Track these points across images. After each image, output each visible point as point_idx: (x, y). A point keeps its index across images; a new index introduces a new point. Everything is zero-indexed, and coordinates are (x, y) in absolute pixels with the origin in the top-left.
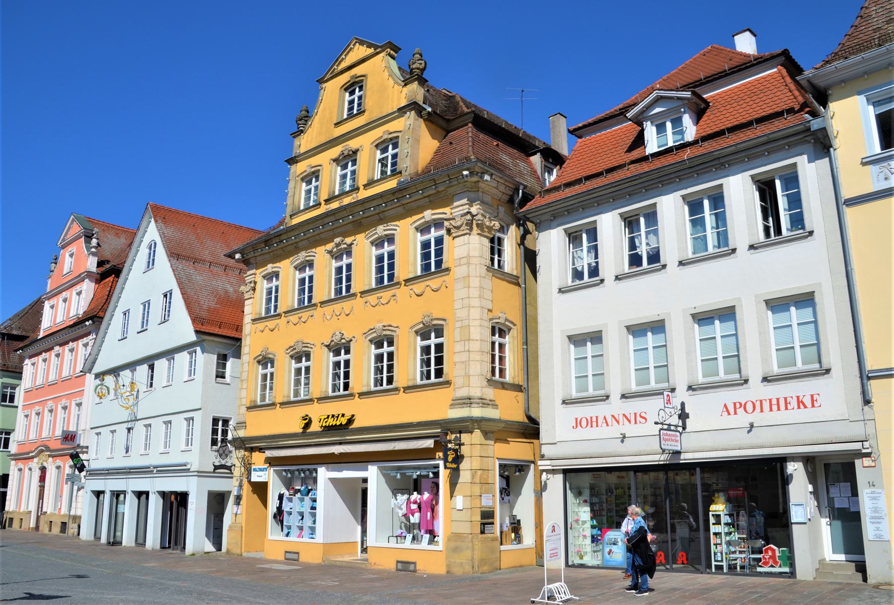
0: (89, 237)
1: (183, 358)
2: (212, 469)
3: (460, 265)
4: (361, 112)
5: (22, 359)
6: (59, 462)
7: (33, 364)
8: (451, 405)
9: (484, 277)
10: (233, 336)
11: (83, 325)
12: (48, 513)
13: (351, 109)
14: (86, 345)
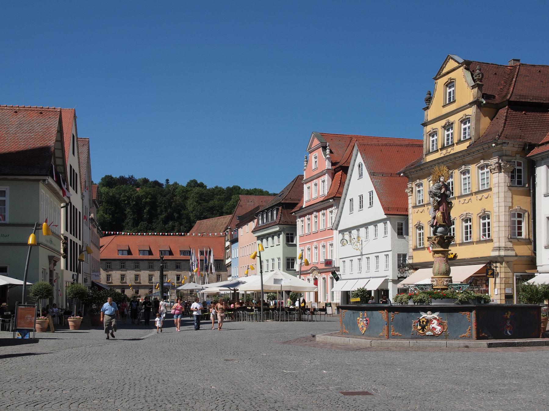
0: (324, 148)
1: (381, 226)
2: (397, 278)
3: (495, 187)
4: (454, 101)
5: (295, 218)
6: (324, 275)
7: (302, 221)
8: (493, 250)
9: (507, 192)
10: (404, 214)
11: (328, 201)
12: (321, 302)
13: (450, 99)
14: (331, 212)
